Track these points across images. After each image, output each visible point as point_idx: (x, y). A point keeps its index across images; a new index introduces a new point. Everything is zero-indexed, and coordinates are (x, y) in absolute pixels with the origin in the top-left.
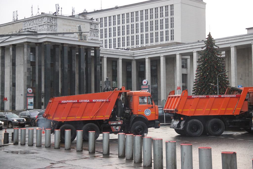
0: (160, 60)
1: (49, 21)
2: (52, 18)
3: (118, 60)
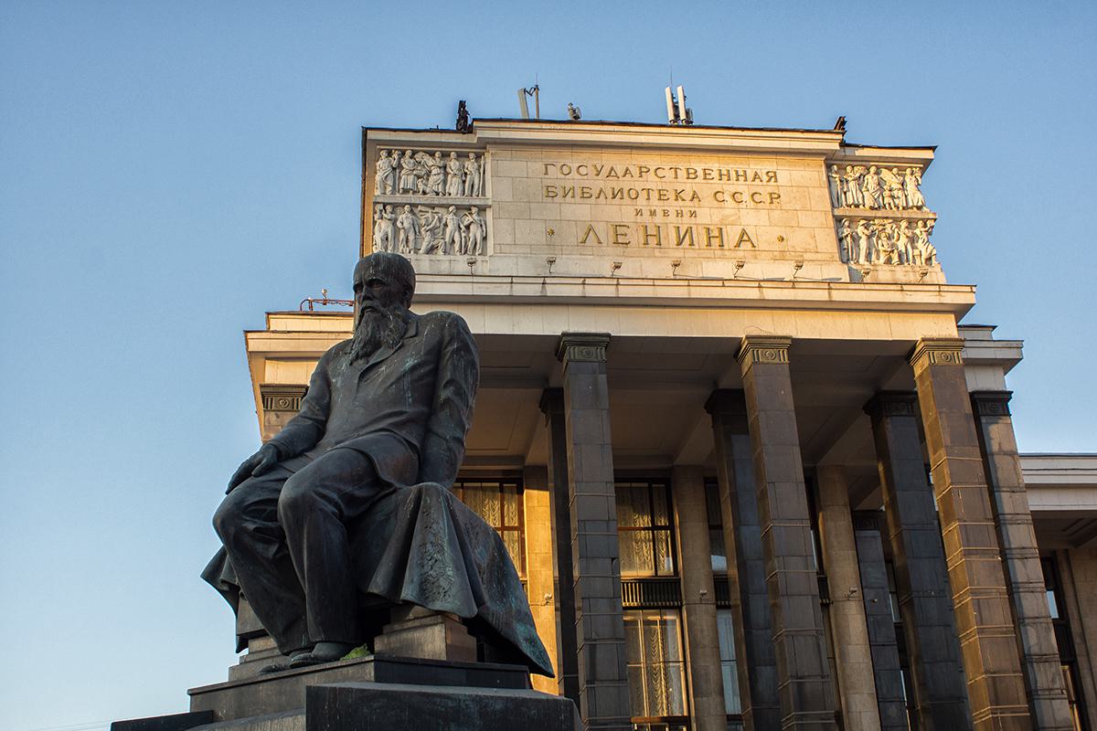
2: (445, 155)
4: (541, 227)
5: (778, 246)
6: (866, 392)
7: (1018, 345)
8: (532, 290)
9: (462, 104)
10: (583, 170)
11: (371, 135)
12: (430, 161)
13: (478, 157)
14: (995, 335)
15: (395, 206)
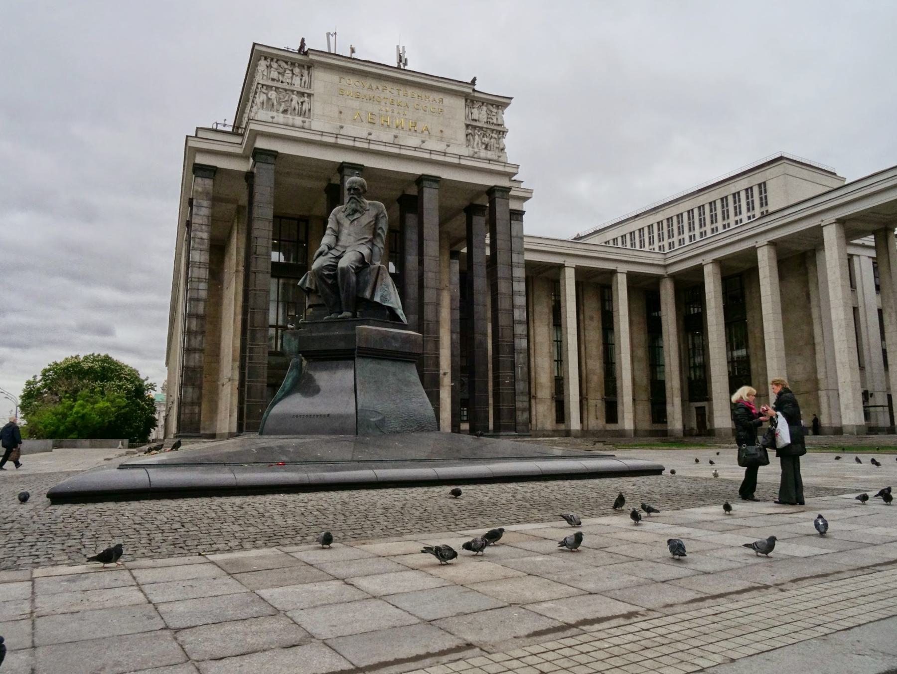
0: (755, 270)
1: (274, 74)
3: (615, 278)
4: (336, 110)
5: (439, 134)
6: (466, 203)
7: (531, 192)
8: (332, 140)
9: (303, 40)
10: (357, 84)
11: (256, 47)
12: (286, 66)
13: (309, 68)
14: (523, 186)
15: (268, 86)
